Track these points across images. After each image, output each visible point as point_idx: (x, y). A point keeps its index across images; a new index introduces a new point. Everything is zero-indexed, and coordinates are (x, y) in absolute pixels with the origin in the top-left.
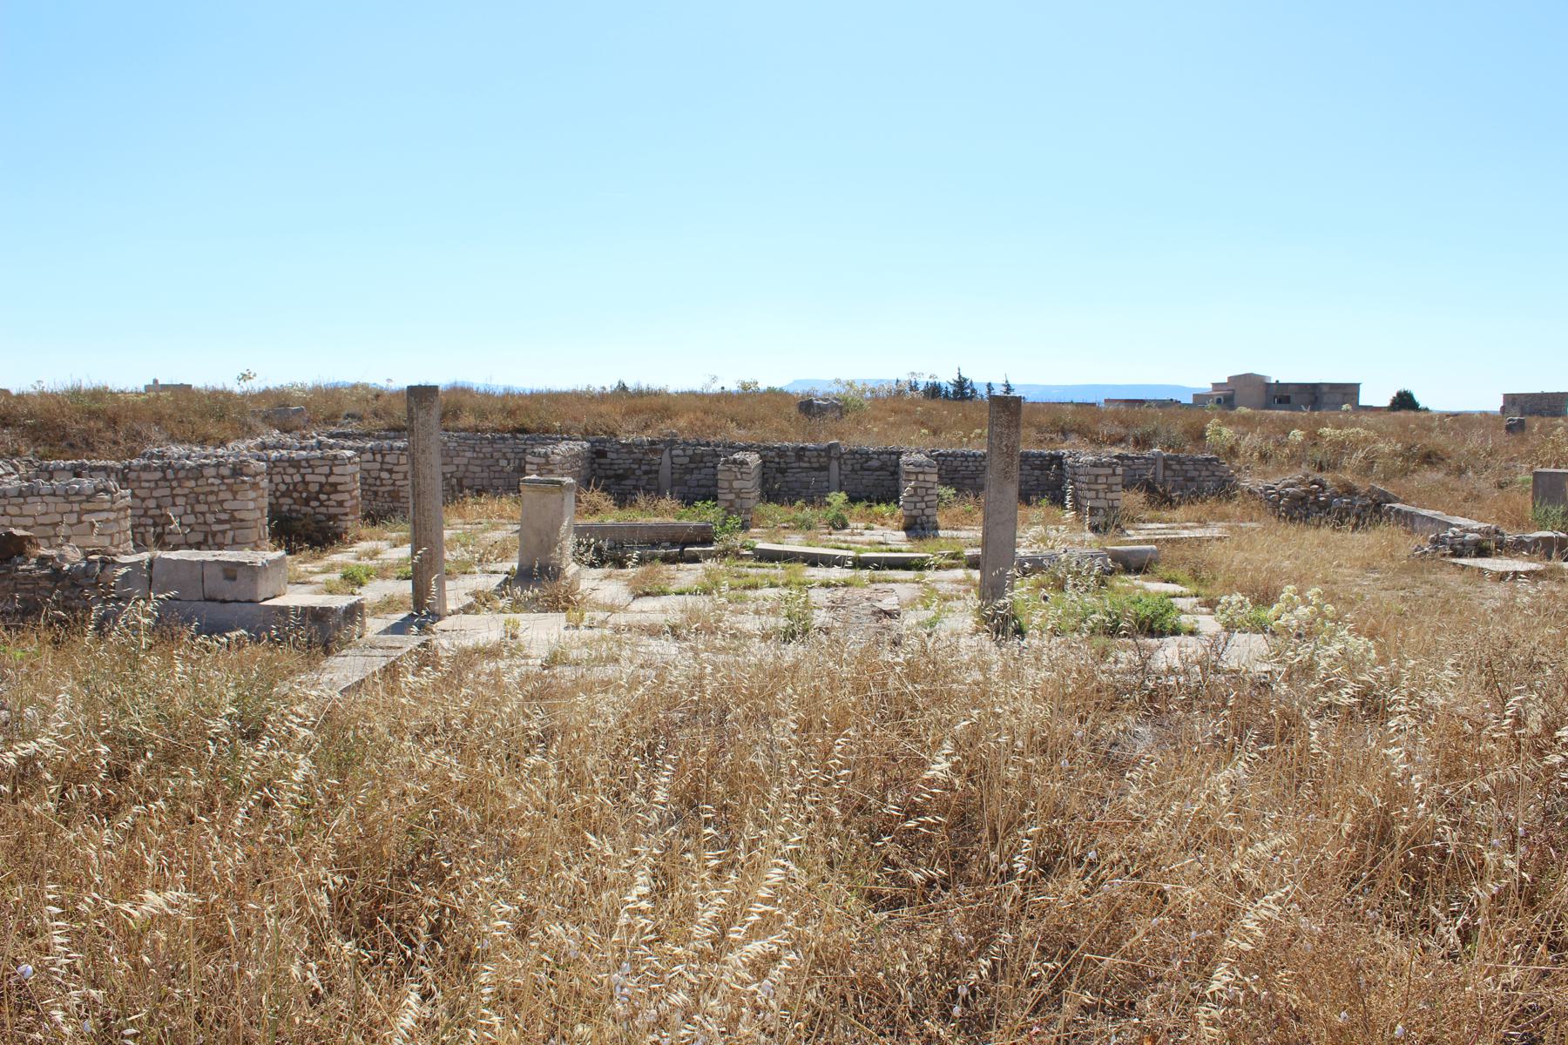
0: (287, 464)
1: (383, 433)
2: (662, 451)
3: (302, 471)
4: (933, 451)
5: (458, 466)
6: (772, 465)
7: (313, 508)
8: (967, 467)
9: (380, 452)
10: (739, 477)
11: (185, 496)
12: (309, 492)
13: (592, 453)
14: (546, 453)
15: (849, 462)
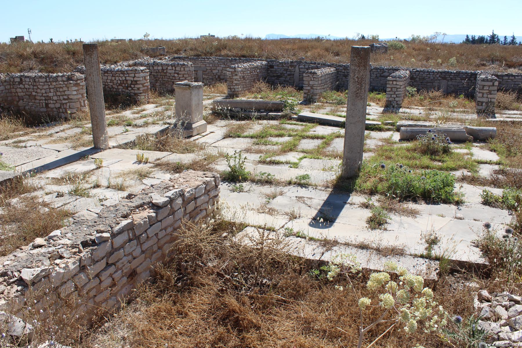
0: (120, 73)
1: (192, 57)
2: (296, 66)
3: (125, 75)
4: (414, 69)
5: (218, 70)
6: (341, 73)
7: (130, 90)
8: (429, 77)
9: (174, 66)
10: (313, 79)
11: (53, 88)
12: (128, 84)
13: (268, 66)
14: (235, 67)
15: (375, 73)
